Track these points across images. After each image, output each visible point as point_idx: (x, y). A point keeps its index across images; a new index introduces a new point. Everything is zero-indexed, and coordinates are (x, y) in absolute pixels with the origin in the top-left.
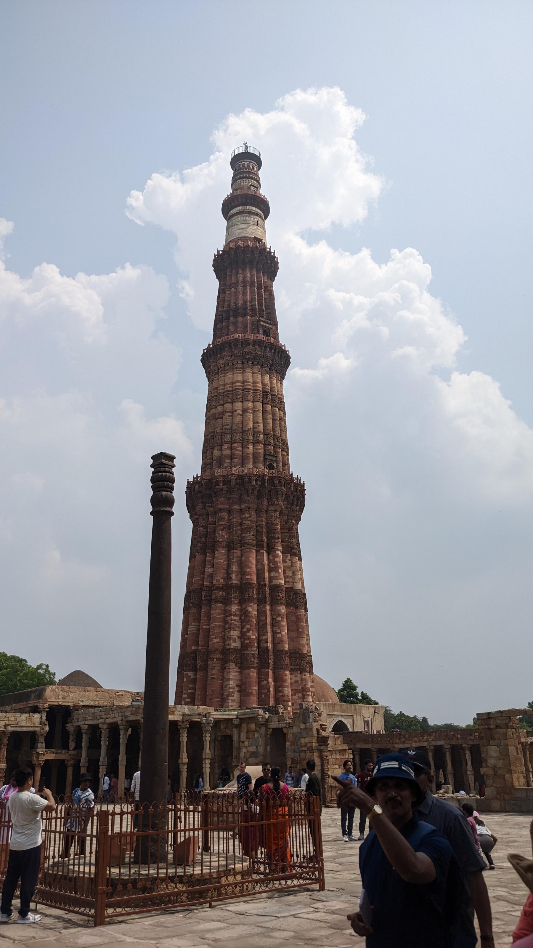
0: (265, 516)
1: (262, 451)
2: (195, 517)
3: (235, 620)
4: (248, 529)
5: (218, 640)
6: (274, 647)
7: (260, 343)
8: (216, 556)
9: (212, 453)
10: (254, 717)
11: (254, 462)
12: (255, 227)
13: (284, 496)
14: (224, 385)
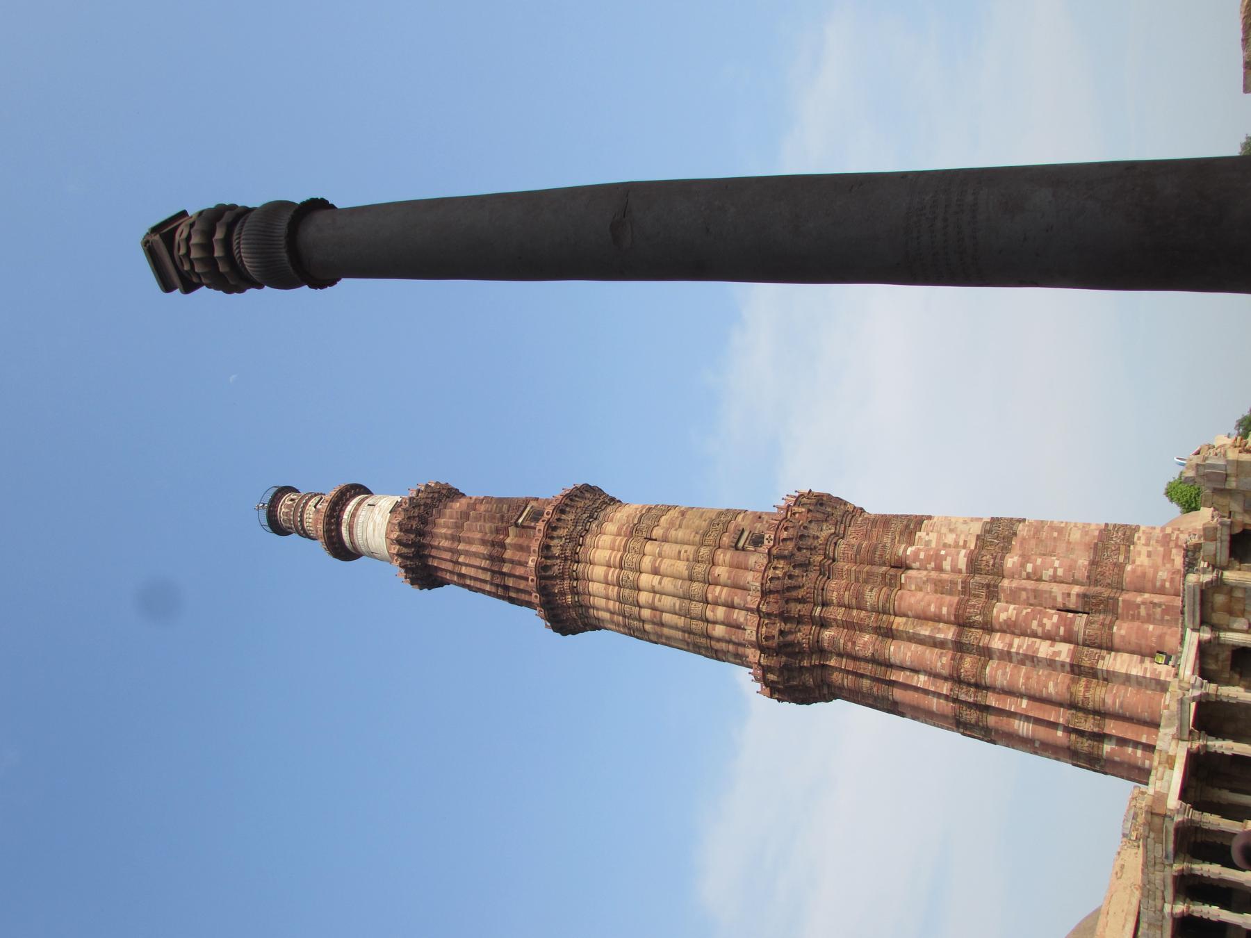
0: (841, 564)
1: (729, 554)
2: (825, 691)
3: (1019, 647)
4: (859, 596)
5: (1051, 684)
6: (1082, 584)
7: (551, 527)
8: (898, 662)
9: (719, 640)
10: (1202, 592)
11: (746, 569)
12: (376, 509)
13: (813, 525)
14: (608, 598)
